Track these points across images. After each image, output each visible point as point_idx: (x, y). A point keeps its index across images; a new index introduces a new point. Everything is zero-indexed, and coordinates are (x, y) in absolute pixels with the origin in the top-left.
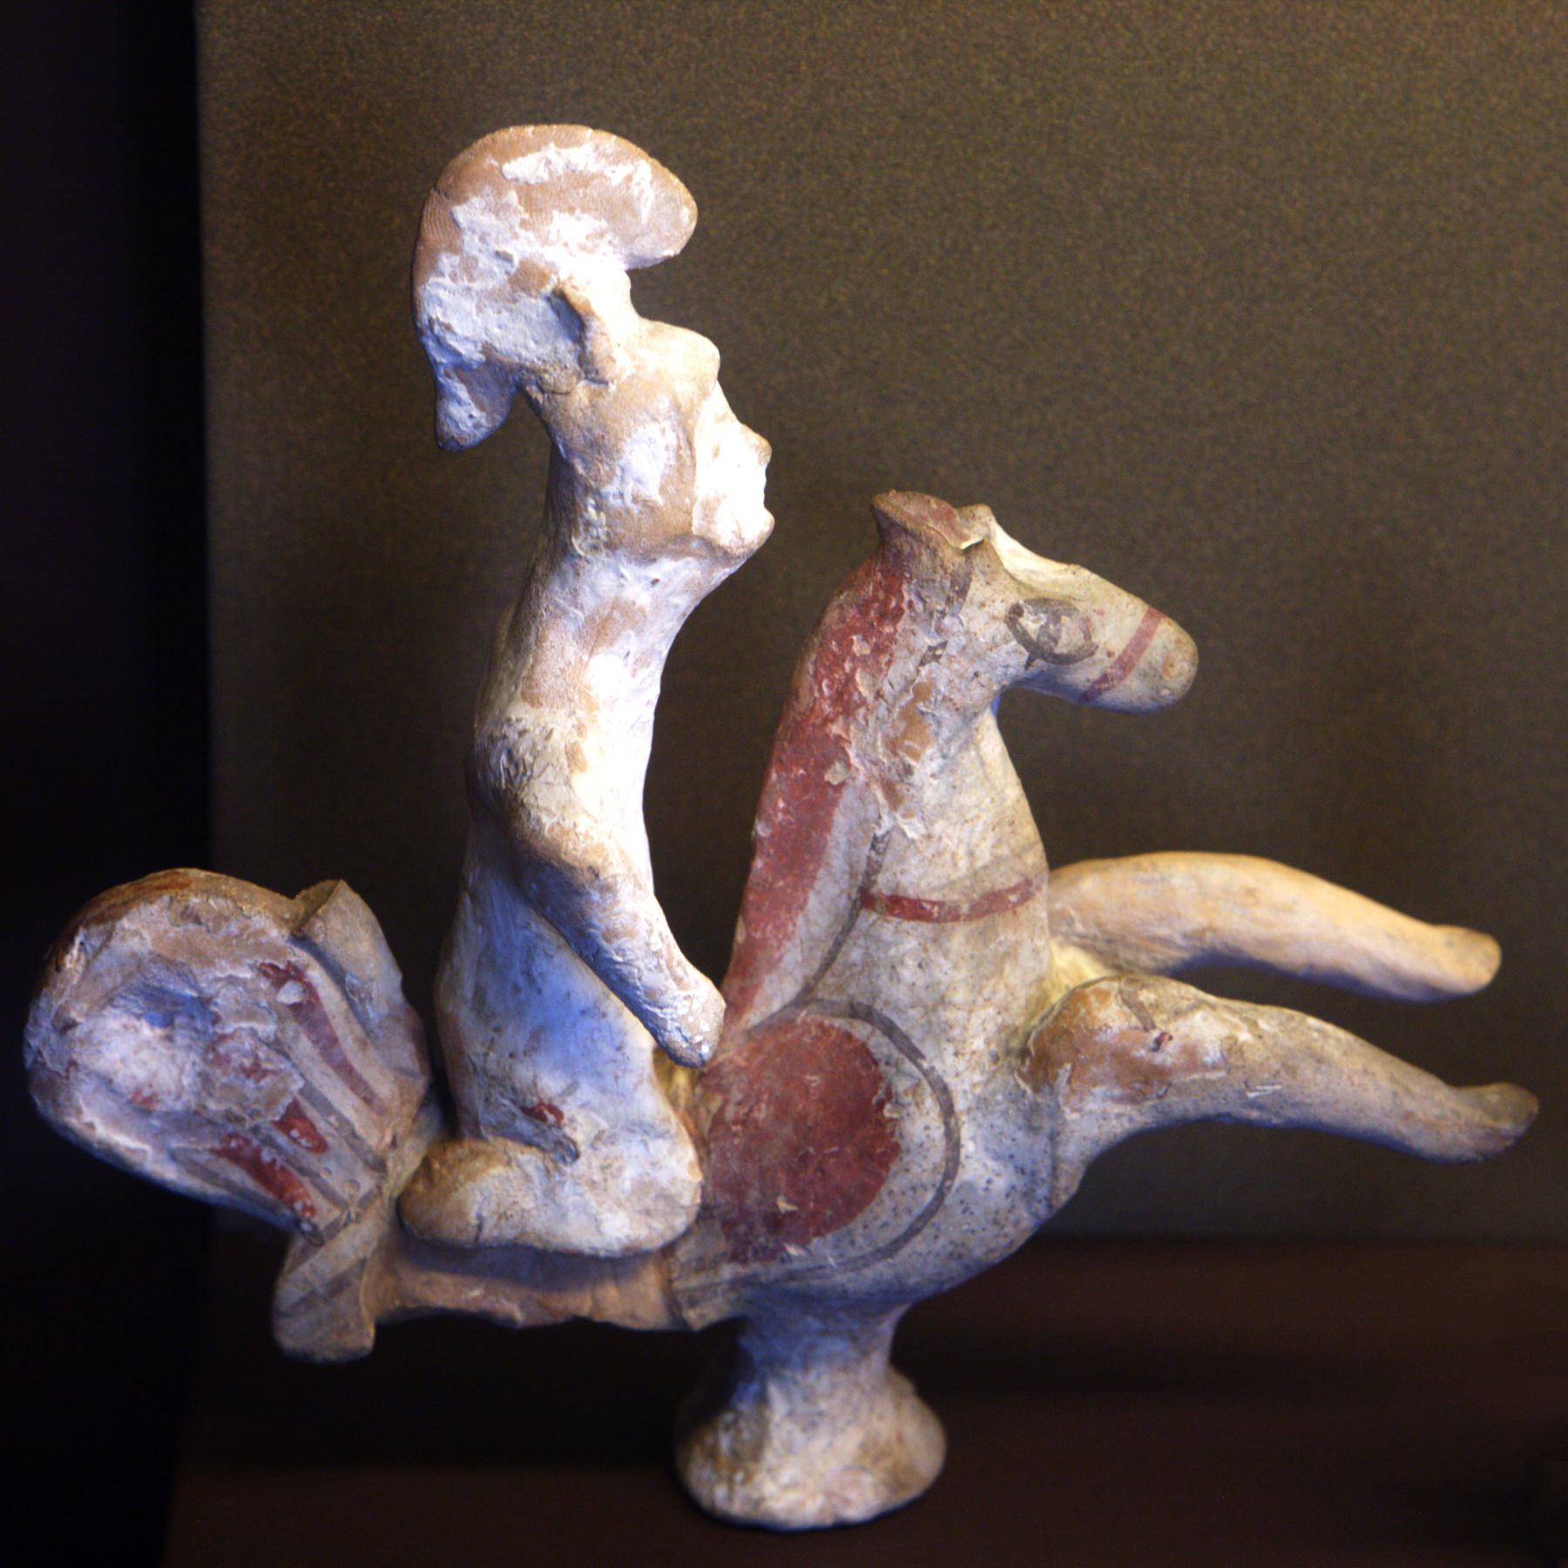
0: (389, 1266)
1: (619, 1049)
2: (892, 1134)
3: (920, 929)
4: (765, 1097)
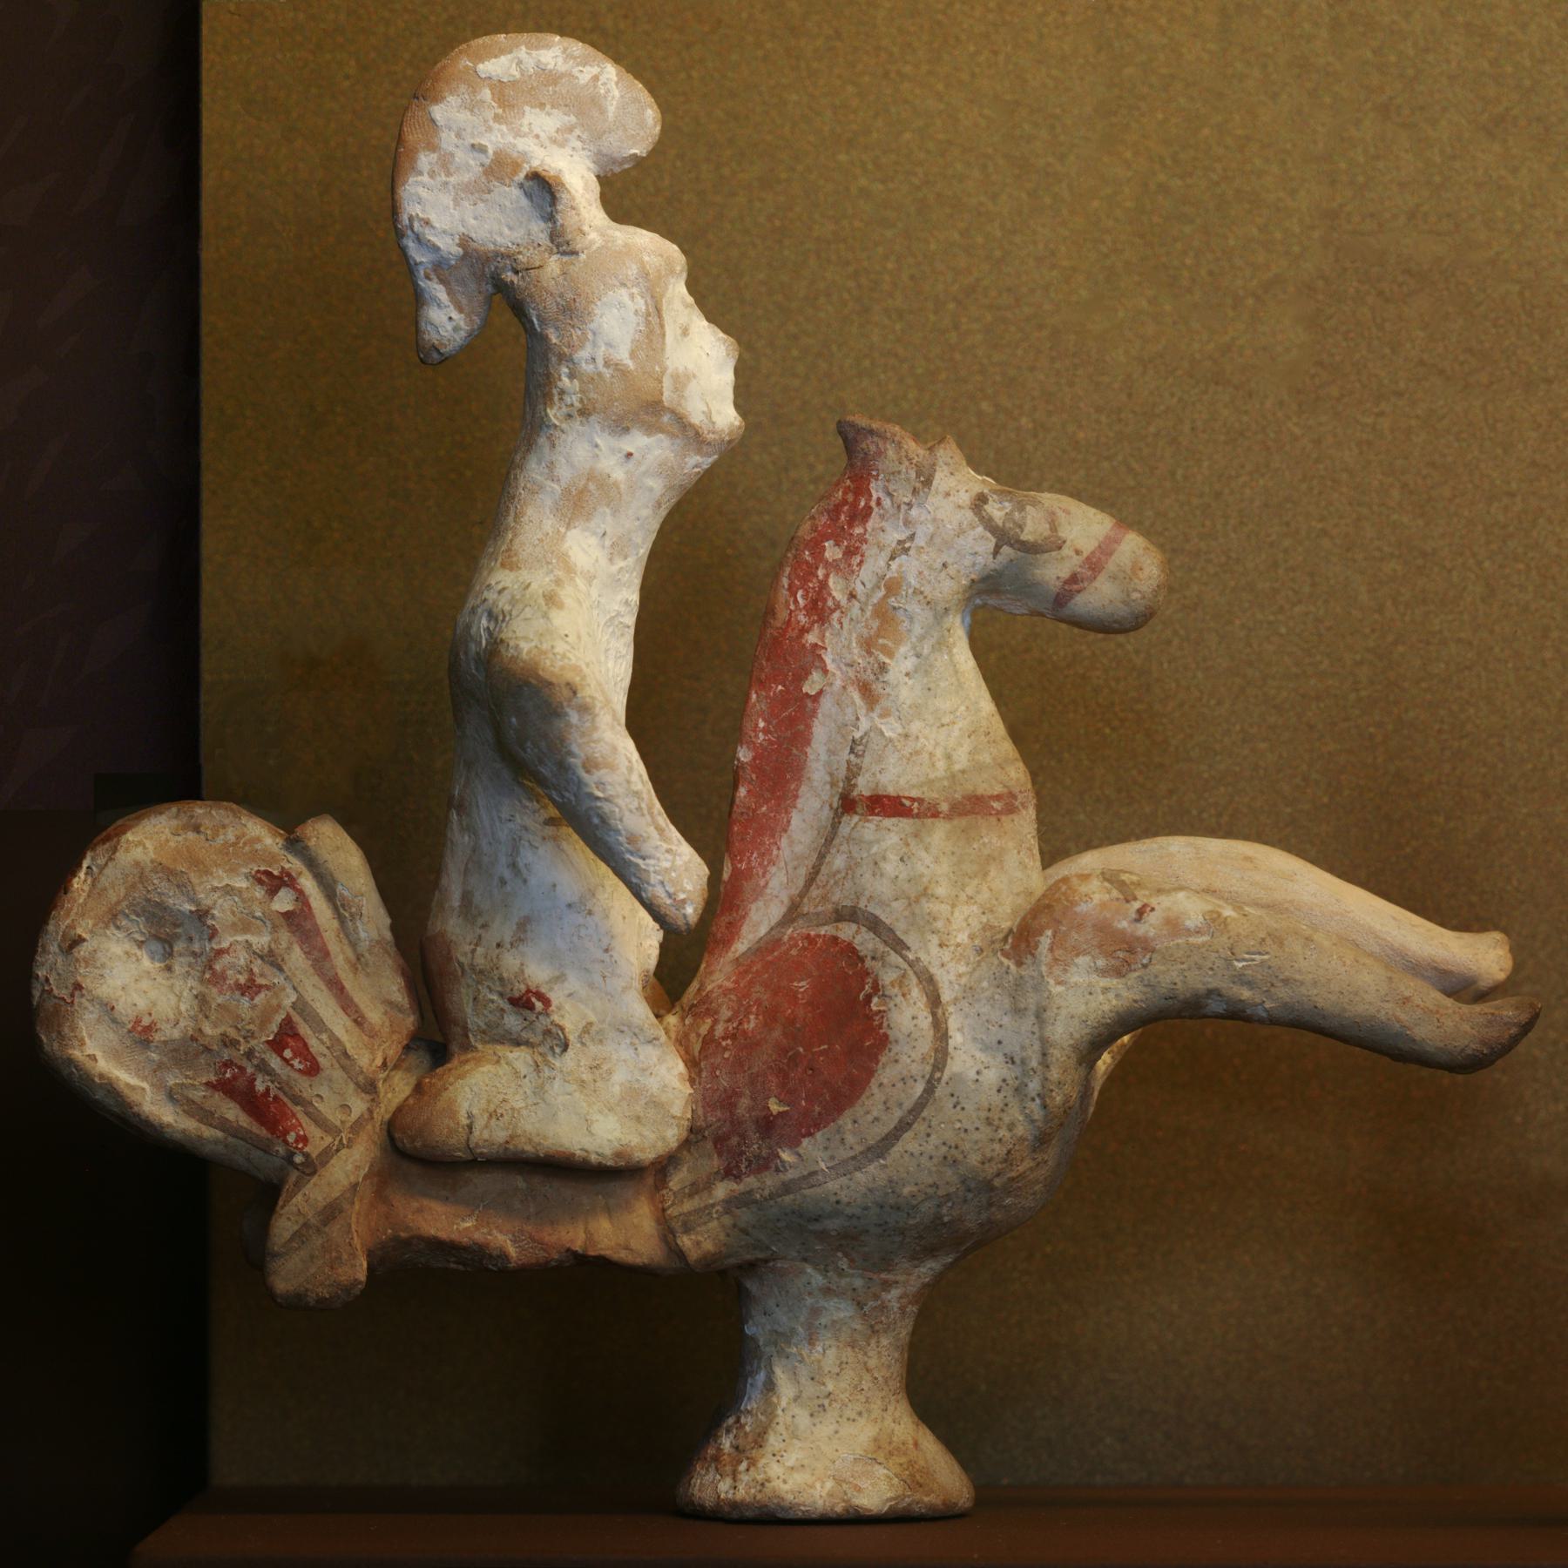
0: (380, 1195)
1: (606, 951)
2: (880, 1026)
3: (901, 825)
4: (754, 1009)
